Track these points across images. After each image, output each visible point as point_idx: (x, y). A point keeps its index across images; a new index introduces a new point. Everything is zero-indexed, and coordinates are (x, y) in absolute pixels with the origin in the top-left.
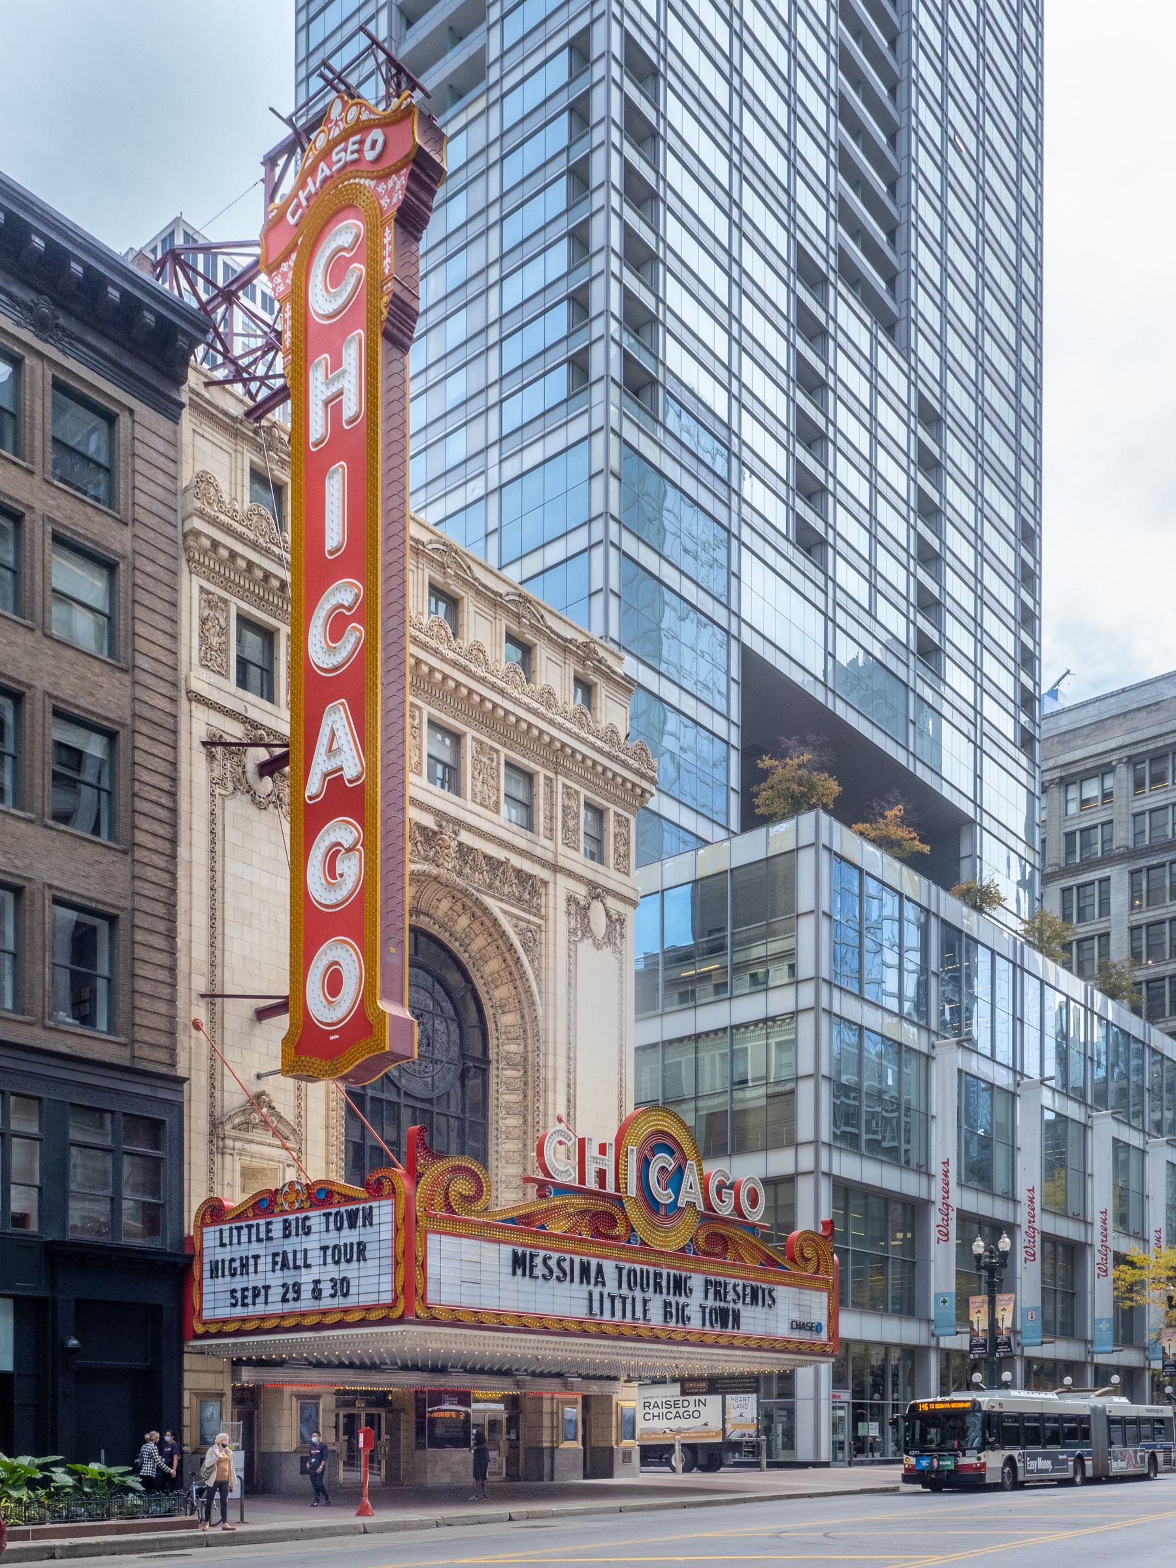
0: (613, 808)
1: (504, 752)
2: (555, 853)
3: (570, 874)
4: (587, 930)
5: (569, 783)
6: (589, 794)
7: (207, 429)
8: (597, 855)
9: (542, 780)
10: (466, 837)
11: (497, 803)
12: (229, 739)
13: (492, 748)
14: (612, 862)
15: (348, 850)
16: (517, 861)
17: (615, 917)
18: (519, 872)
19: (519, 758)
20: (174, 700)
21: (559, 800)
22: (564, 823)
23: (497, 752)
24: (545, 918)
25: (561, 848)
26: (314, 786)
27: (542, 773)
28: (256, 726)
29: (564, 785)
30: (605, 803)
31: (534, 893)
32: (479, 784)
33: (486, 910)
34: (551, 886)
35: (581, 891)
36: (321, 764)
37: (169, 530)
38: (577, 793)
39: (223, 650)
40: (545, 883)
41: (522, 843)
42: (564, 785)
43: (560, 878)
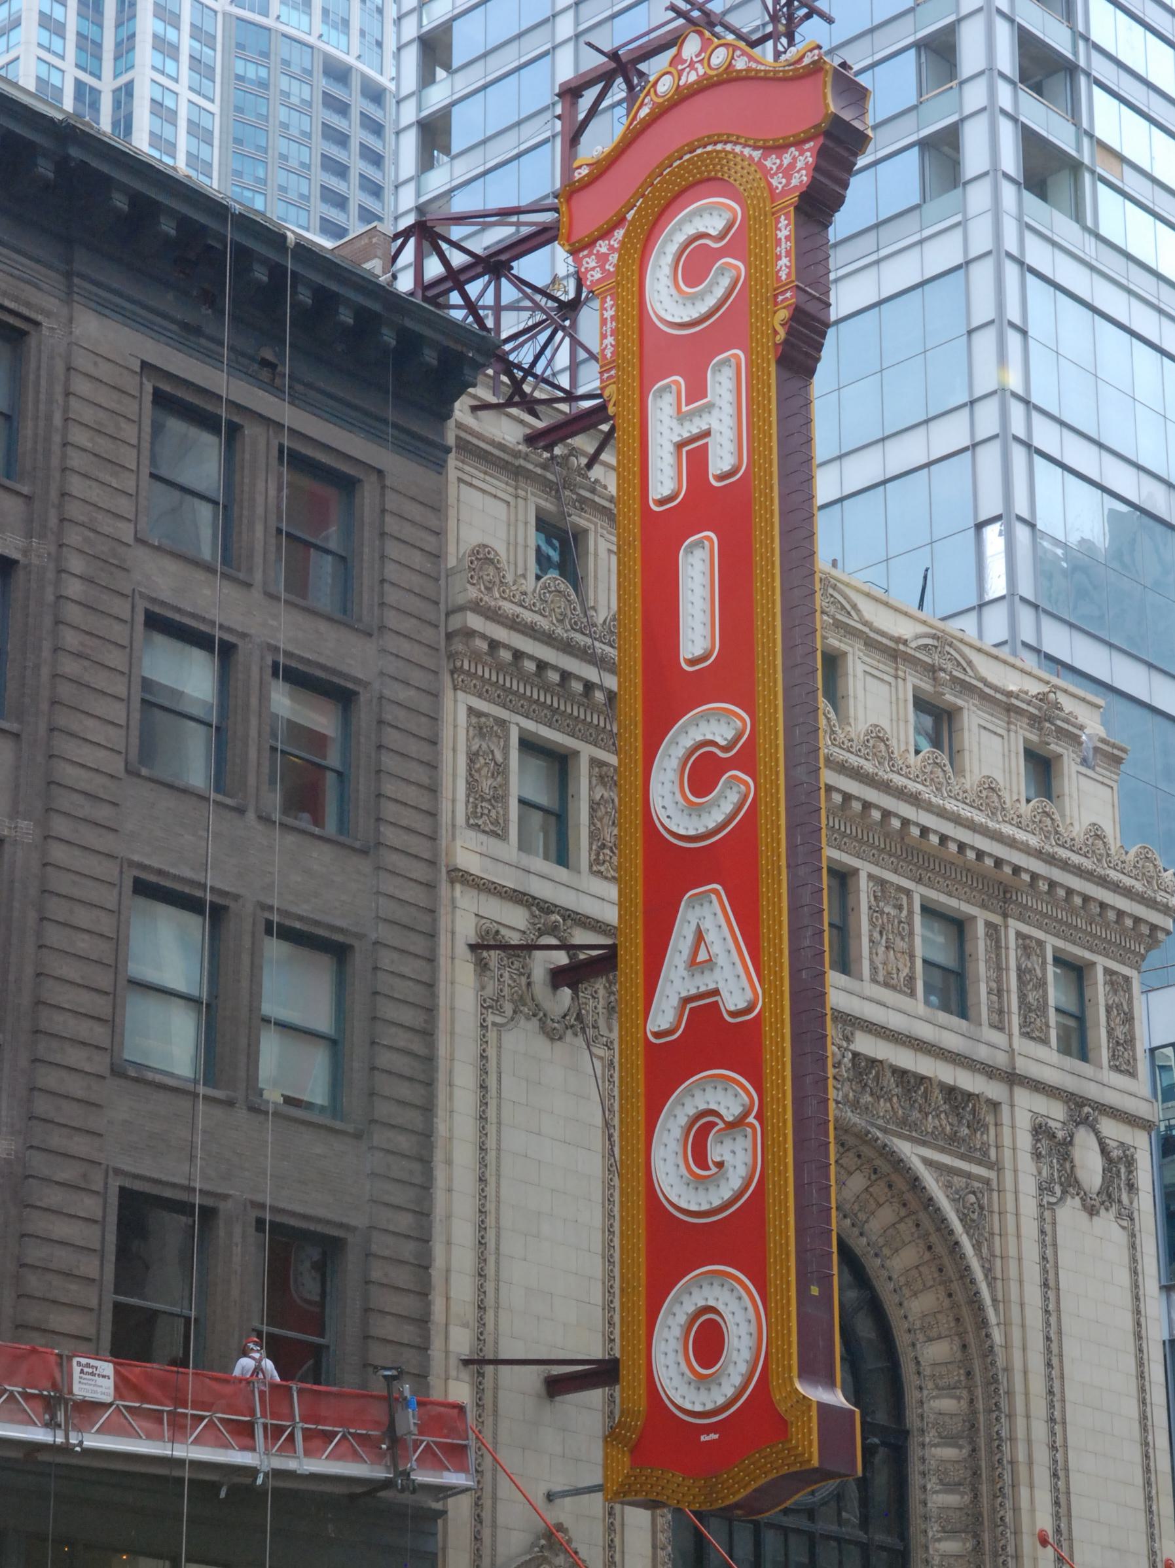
0: (1101, 962)
1: (920, 891)
2: (1011, 1052)
3: (1038, 1086)
4: (1070, 1182)
5: (1025, 929)
6: (1060, 944)
7: (473, 471)
8: (1077, 1044)
9: (981, 929)
10: (865, 1045)
11: (911, 979)
12: (515, 939)
13: (900, 889)
14: (1105, 1055)
15: (731, 1125)
16: (946, 1073)
17: (1115, 1154)
18: (951, 1092)
19: (943, 898)
20: (431, 887)
21: (1012, 959)
22: (1022, 997)
23: (908, 893)
24: (997, 1166)
25: (1019, 1043)
26: (664, 1015)
27: (981, 917)
28: (547, 908)
29: (1019, 934)
30: (1087, 955)
31: (977, 1125)
32: (881, 949)
33: (899, 1164)
34: (1005, 1109)
35: (1056, 1112)
36: (676, 984)
37: (428, 635)
38: (1041, 943)
39: (499, 797)
40: (995, 1105)
41: (952, 1042)
42: (1019, 934)
43: (1022, 1096)
